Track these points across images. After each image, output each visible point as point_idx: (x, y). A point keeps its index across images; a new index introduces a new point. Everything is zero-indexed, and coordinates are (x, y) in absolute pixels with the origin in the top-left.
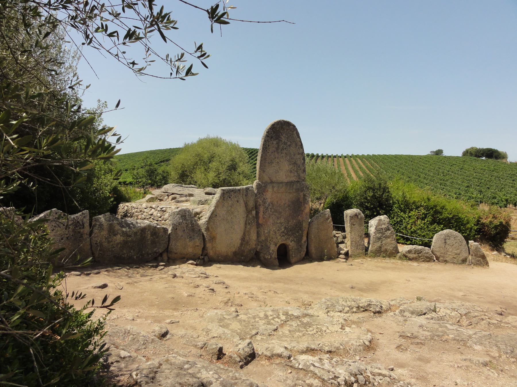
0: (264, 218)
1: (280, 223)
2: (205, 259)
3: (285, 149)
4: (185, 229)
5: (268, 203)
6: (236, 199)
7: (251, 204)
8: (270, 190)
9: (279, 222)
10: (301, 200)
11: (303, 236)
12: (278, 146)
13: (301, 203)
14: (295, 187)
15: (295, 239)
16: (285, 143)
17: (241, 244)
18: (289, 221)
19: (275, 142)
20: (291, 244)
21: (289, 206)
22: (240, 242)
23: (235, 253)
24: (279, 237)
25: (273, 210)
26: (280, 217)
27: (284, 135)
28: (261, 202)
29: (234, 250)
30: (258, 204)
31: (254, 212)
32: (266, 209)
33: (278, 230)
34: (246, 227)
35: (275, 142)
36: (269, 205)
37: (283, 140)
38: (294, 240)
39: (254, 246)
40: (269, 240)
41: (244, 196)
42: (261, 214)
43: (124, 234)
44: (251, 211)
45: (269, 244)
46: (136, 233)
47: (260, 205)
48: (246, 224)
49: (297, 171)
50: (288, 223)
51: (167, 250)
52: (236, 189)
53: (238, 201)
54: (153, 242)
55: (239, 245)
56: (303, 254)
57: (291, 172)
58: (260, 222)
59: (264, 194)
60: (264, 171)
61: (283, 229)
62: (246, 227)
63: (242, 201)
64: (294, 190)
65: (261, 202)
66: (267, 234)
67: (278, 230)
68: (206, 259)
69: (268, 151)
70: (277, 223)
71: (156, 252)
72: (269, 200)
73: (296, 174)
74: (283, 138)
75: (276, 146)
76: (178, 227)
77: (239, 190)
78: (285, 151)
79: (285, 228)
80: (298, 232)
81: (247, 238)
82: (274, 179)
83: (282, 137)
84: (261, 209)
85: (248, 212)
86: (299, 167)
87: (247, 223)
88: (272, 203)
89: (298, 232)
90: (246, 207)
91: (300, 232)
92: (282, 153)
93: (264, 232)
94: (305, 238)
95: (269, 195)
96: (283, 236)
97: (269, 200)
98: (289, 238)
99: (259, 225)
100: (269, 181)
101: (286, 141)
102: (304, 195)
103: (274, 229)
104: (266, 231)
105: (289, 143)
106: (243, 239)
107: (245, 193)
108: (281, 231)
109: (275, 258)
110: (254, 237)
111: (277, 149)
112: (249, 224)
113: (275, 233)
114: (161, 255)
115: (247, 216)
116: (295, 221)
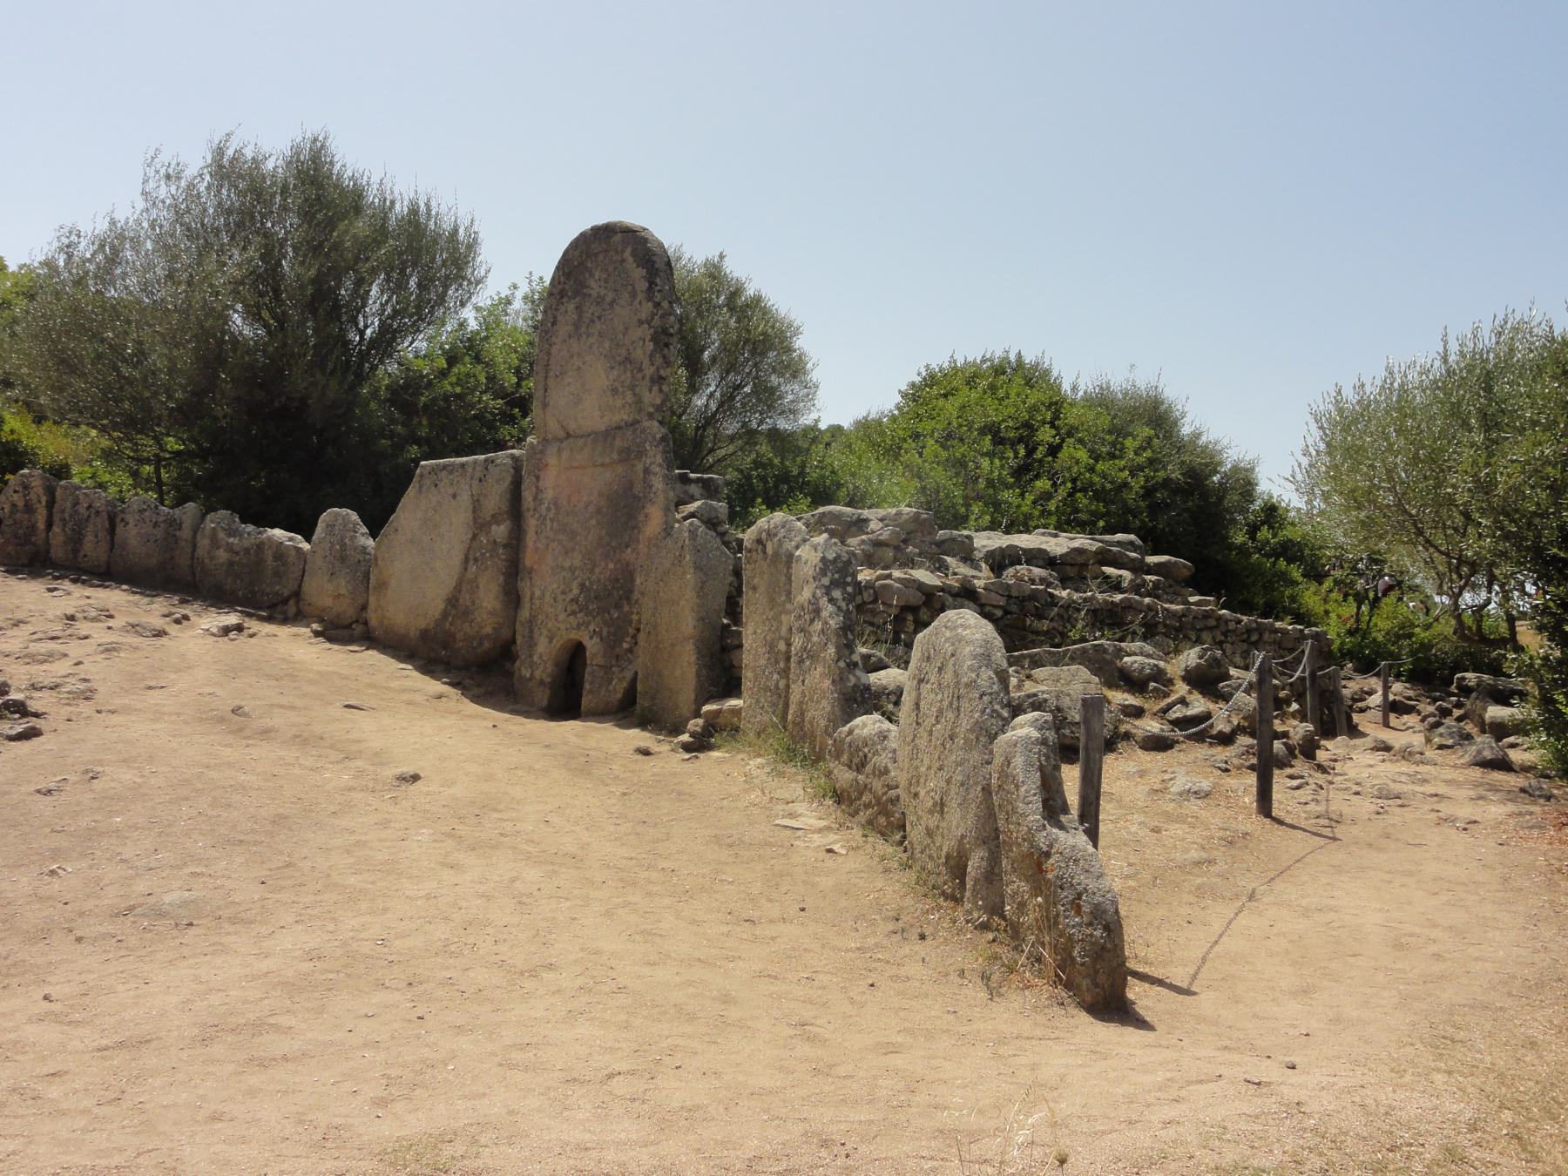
0: (537, 549)
2: (345, 629)
8: (552, 460)
9: (567, 564)
10: (638, 488)
12: (580, 317)
13: (639, 499)
14: (618, 443)
15: (605, 633)
16: (599, 301)
17: (445, 615)
18: (595, 566)
19: (571, 307)
21: (599, 511)
22: (442, 606)
23: (424, 635)
24: (562, 616)
26: (573, 549)
27: (597, 274)
29: (423, 624)
31: (501, 531)
33: (563, 593)
36: (548, 510)
38: (599, 634)
42: (530, 538)
43: (230, 548)
46: (247, 550)
48: (466, 560)
49: (632, 388)
50: (592, 571)
52: (453, 465)
53: (454, 496)
54: (277, 574)
55: (437, 615)
57: (614, 391)
61: (576, 591)
63: (465, 499)
64: (615, 457)
67: (563, 593)
68: (358, 629)
70: (563, 569)
71: (277, 593)
73: (630, 398)
74: (595, 287)
77: (463, 465)
78: (598, 325)
79: (582, 585)
80: (618, 606)
82: (572, 427)
85: (480, 525)
86: (640, 370)
88: (556, 504)
89: (618, 606)
90: (474, 511)
91: (626, 608)
96: (574, 613)
97: (549, 495)
98: (589, 624)
100: (562, 434)
102: (647, 471)
104: (537, 593)
105: (610, 296)
106: (452, 601)
107: (478, 475)
109: (542, 683)
110: (488, 598)
111: (577, 326)
112: (476, 560)
114: (285, 601)
115: (475, 537)
116: (611, 566)
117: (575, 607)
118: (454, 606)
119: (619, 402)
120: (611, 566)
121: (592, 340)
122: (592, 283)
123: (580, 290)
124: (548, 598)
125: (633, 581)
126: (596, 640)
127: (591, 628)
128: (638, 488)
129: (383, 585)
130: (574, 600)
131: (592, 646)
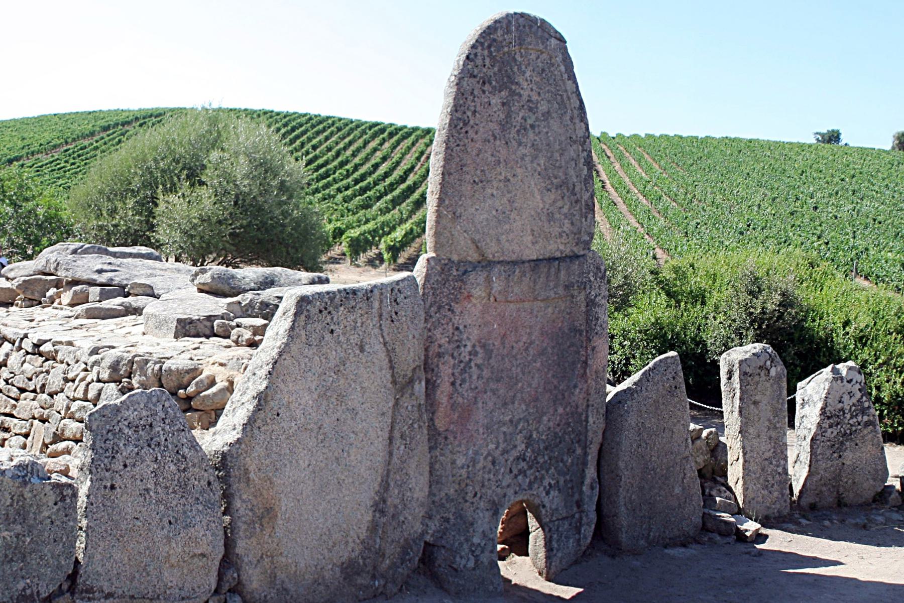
1: (511, 421)
3: (532, 126)
4: (151, 486)
5: (469, 348)
6: (354, 339)
7: (410, 355)
8: (478, 292)
11: (585, 464)
12: (508, 116)
15: (561, 483)
19: (495, 100)
20: (546, 501)
21: (543, 353)
24: (507, 480)
25: (486, 373)
27: (528, 74)
28: (444, 341)
29: (344, 554)
30: (434, 349)
31: (420, 388)
32: (463, 371)
34: (391, 454)
35: (495, 100)
36: (473, 353)
37: (525, 94)
39: (418, 528)
40: (469, 497)
41: (385, 323)
42: (443, 394)
44: (411, 382)
45: (469, 513)
47: (440, 355)
48: (391, 439)
56: (588, 531)
57: (550, 217)
58: (440, 424)
59: (457, 308)
60: (456, 217)
62: (391, 454)
63: (376, 346)
65: (444, 341)
66: (463, 472)
67: (505, 452)
69: (471, 134)
72: (475, 333)
75: (502, 116)
76: (118, 483)
80: (571, 451)
81: (393, 498)
82: (492, 251)
83: (520, 79)
84: (446, 370)
85: (401, 386)
87: (397, 434)
88: (483, 346)
89: (571, 451)
90: (392, 368)
91: (579, 451)
92: (520, 144)
93: (453, 462)
94: (591, 472)
95: (475, 313)
96: (522, 472)
98: (542, 478)
99: (435, 438)
101: (535, 98)
103: (492, 446)
105: (543, 107)
107: (388, 309)
108: (515, 453)
110: (418, 486)
111: (504, 125)
113: (493, 463)
115: (397, 403)
117: (523, 465)
118: (382, 512)
119: (556, 230)
120: (560, 410)
121: (522, 150)
123: (507, 82)
127: (546, 483)
130: (521, 458)
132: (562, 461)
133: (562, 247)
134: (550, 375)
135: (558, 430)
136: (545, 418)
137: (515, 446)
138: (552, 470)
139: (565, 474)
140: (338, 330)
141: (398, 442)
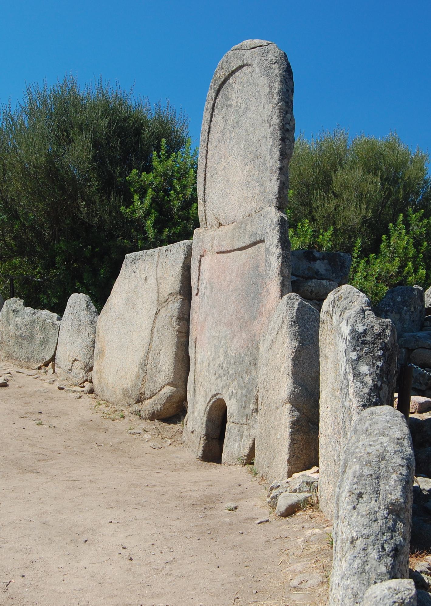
17: (138, 377)
31: (174, 306)
51: (53, 359)
63: (152, 281)
67: (214, 359)
73: (258, 189)
80: (248, 371)
86: (264, 164)
89: (248, 371)
106: (144, 366)
110: (166, 363)
120: (244, 335)
121: (233, 143)
122: (233, 96)
124: (205, 364)
125: (258, 349)
126: (234, 401)
128: (262, 268)
129: (102, 351)
131: (232, 407)
132: (242, 378)
133: (254, 205)
134: (240, 307)
135: (241, 351)
136: (235, 340)
137: (219, 357)
138: (235, 383)
139: (242, 388)
140: (137, 272)
141: (155, 334)
